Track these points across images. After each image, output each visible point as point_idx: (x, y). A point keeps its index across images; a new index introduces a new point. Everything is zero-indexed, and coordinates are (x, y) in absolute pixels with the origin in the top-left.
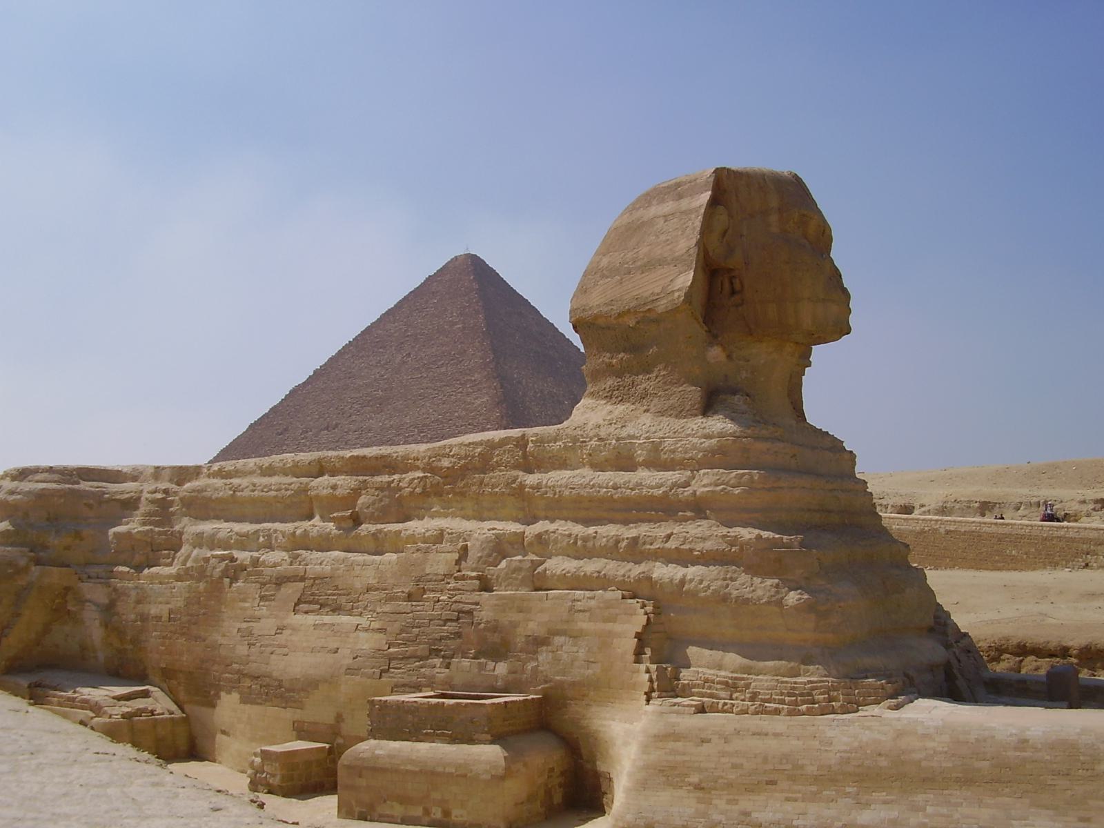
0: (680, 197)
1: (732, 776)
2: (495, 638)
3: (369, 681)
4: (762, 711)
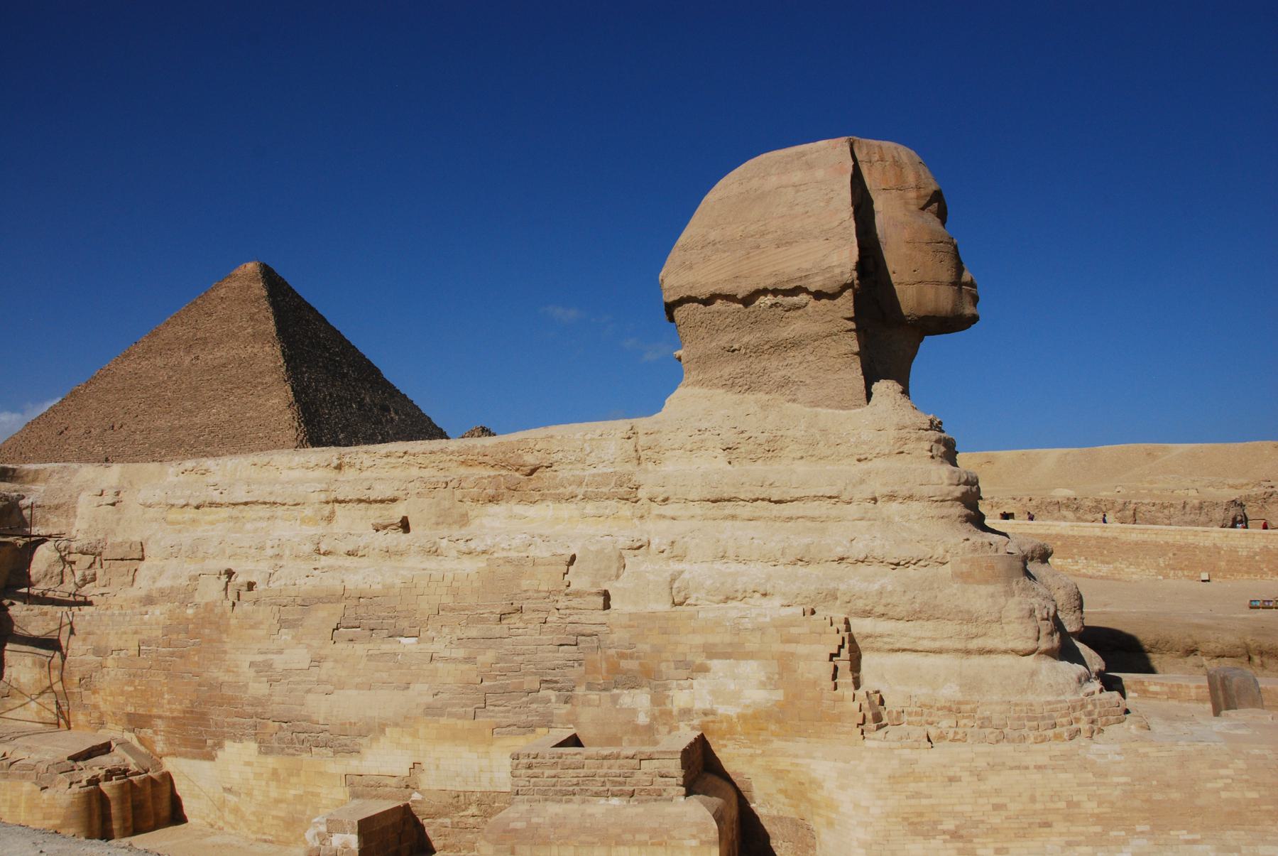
0: (810, 166)
1: (996, 820)
3: (460, 722)
4: (1002, 738)
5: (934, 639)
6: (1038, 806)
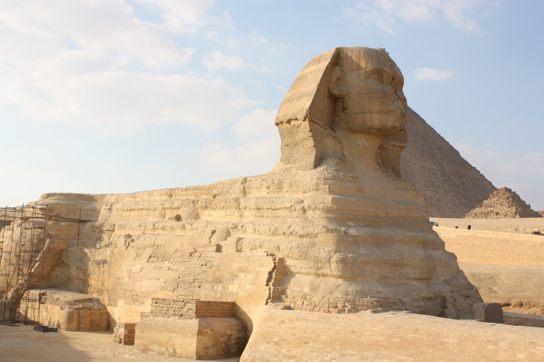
0: (319, 62)
1: (290, 339)
2: (218, 274)
5: (306, 269)
6: (306, 335)
